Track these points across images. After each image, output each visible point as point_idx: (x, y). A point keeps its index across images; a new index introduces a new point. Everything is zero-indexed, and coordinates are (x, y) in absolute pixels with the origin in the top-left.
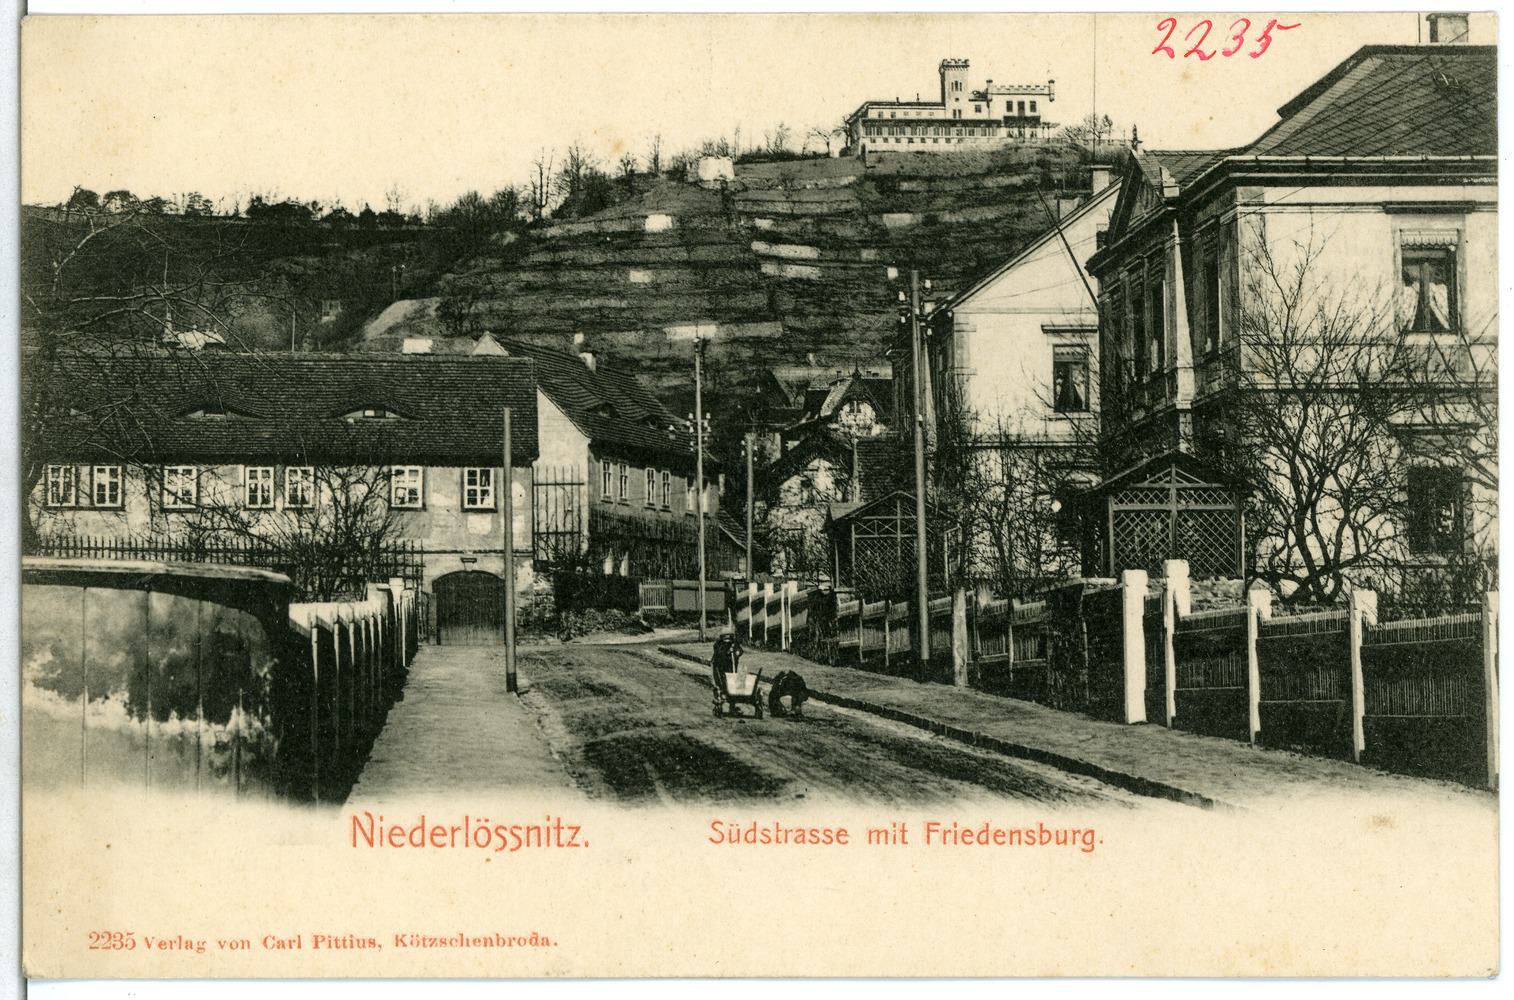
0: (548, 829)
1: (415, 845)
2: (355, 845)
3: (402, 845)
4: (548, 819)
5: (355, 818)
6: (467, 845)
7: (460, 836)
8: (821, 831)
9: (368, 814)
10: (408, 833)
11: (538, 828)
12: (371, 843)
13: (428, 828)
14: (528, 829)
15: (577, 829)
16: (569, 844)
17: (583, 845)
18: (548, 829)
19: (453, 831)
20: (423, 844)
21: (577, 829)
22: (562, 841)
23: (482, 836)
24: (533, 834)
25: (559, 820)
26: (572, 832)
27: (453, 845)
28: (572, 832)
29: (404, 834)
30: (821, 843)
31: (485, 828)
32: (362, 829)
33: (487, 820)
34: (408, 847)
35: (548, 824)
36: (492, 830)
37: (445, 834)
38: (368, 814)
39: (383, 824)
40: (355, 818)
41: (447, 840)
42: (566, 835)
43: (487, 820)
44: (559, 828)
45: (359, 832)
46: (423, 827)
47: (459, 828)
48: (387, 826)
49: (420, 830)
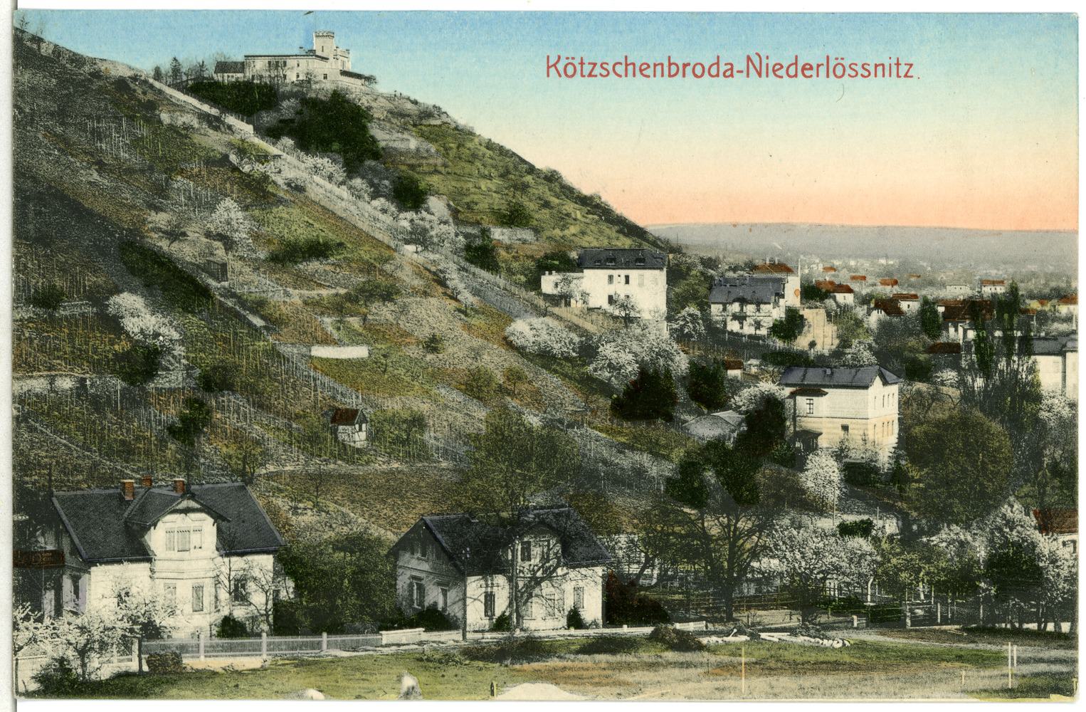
1: (790, 76)
2: (548, 76)
5: (749, 58)
7: (823, 70)
9: (757, 54)
10: (785, 69)
12: (760, 74)
14: (876, 66)
15: (911, 65)
16: (906, 76)
19: (818, 66)
20: (796, 76)
21: (911, 65)
23: (839, 71)
24: (880, 68)
25: (898, 59)
26: (908, 67)
27: (818, 76)
28: (908, 67)
31: (842, 65)
33: (842, 59)
35: (889, 61)
37: (811, 68)
38: (757, 54)
39: (769, 61)
40: (749, 58)
41: (814, 73)
42: (903, 71)
43: (842, 59)
44: (898, 64)
45: (750, 64)
46: (796, 64)
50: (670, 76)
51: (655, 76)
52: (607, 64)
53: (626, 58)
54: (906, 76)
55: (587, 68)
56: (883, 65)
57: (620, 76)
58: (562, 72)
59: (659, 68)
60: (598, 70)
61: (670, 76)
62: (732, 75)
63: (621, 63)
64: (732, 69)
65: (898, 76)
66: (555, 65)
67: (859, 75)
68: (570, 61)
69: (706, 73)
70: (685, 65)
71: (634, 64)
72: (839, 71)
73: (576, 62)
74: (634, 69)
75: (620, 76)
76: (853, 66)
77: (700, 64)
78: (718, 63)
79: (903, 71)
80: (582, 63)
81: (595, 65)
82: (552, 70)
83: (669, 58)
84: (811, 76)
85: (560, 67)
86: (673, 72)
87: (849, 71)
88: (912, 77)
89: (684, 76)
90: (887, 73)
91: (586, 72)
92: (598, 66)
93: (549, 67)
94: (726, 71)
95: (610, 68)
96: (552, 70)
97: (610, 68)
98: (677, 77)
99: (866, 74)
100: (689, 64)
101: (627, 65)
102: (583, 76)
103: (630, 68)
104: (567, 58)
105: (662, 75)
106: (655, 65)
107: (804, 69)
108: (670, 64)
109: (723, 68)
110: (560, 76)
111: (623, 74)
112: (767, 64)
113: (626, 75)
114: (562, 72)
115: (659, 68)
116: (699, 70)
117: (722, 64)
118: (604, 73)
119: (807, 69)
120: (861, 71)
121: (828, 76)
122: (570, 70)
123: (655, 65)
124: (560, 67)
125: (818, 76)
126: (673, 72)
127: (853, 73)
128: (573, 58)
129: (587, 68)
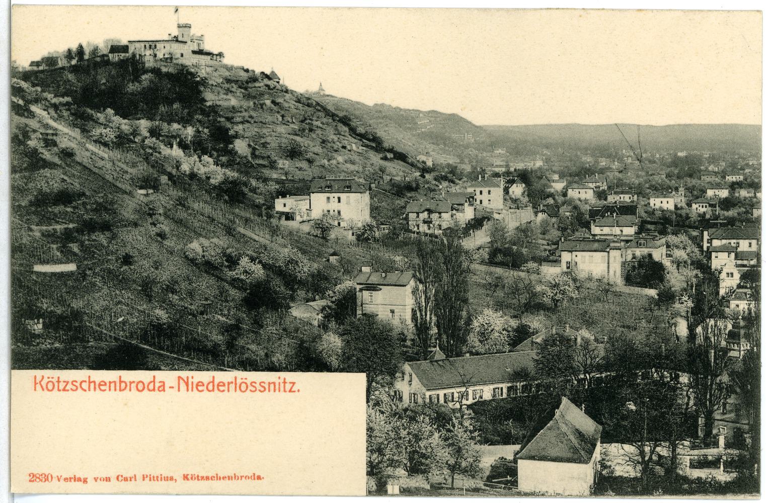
0: (279, 383)
3: (203, 391)
4: (279, 378)
6: (35, 390)
7: (232, 386)
8: (258, 383)
11: (274, 383)
13: (216, 384)
14: (269, 383)
15: (294, 383)
16: (290, 391)
17: (297, 390)
18: (279, 383)
20: (213, 390)
21: (294, 383)
22: (60, 388)
23: (243, 387)
24: (272, 386)
25: (285, 379)
27: (229, 391)
29: (203, 385)
30: (258, 392)
31: (246, 383)
32: (184, 381)
33: (246, 379)
34: (206, 392)
36: (249, 384)
41: (226, 388)
42: (288, 386)
43: (246, 379)
44: (285, 382)
46: (213, 382)
47: (232, 383)
48: (196, 381)
49: (153, 383)
50: (120, 390)
51: (110, 390)
52: (76, 382)
53: (89, 377)
54: (290, 391)
55: (62, 386)
56: (274, 383)
57: (85, 390)
58: (44, 387)
59: (113, 385)
60: (69, 387)
61: (120, 390)
62: (164, 390)
63: (85, 381)
64: (164, 386)
65: (285, 391)
67: (258, 389)
68: (50, 379)
71: (94, 382)
72: (243, 387)
73: (55, 380)
74: (95, 385)
75: (85, 390)
76: (254, 384)
78: (154, 381)
79: (288, 386)
81: (68, 383)
82: (38, 386)
83: (120, 377)
84: (223, 391)
85: (44, 383)
87: (250, 388)
88: (294, 391)
89: (130, 390)
91: (61, 387)
93: (36, 384)
94: (159, 387)
95: (78, 384)
96: (38, 386)
97: (78, 384)
98: (125, 391)
99: (262, 389)
100: (134, 382)
101: (90, 382)
102: (59, 390)
103: (92, 385)
104: (49, 378)
105: (115, 390)
106: (110, 383)
107: (218, 385)
108: (121, 382)
109: (157, 385)
110: (43, 390)
111: (87, 389)
112: (192, 383)
113: (89, 390)
114: (44, 387)
115: (113, 385)
116: (140, 387)
117: (157, 380)
118: (74, 388)
119: (221, 386)
120: (257, 386)
121: (236, 390)
122: (50, 386)
124: (44, 383)
125: (229, 391)
127: (254, 389)
128: (53, 378)
129: (62, 386)
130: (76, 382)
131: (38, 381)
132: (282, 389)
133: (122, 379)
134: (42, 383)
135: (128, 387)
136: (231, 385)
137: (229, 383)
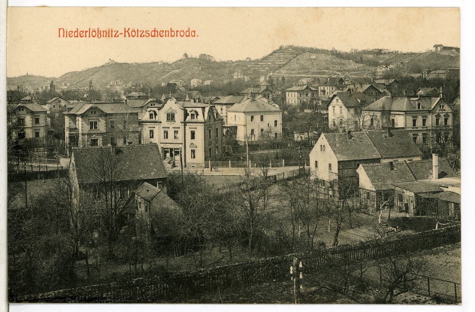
7: (88, 34)
42: (114, 34)
44: (112, 31)
47: (87, 31)
59: (167, 32)
61: (171, 36)
66: (127, 31)
68: (133, 30)
69: (185, 35)
70: (177, 31)
74: (158, 32)
77: (182, 31)
79: (114, 34)
80: (138, 31)
86: (173, 35)
90: (107, 35)
92: (145, 32)
99: (147, 35)
100: (179, 31)
108: (171, 31)
112: (67, 31)
114: (130, 34)
115: (167, 32)
123: (166, 31)
126: (173, 35)
130: (149, 31)
131: (127, 30)
132: (110, 35)
133: (172, 30)
134: (129, 31)
135: (176, 35)
136: (87, 33)
137: (86, 32)
